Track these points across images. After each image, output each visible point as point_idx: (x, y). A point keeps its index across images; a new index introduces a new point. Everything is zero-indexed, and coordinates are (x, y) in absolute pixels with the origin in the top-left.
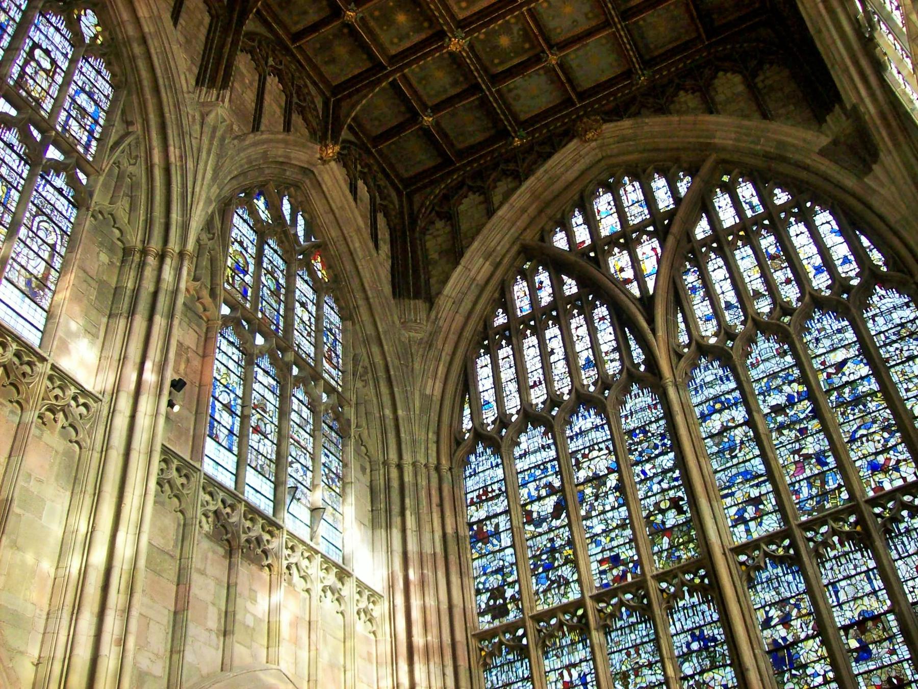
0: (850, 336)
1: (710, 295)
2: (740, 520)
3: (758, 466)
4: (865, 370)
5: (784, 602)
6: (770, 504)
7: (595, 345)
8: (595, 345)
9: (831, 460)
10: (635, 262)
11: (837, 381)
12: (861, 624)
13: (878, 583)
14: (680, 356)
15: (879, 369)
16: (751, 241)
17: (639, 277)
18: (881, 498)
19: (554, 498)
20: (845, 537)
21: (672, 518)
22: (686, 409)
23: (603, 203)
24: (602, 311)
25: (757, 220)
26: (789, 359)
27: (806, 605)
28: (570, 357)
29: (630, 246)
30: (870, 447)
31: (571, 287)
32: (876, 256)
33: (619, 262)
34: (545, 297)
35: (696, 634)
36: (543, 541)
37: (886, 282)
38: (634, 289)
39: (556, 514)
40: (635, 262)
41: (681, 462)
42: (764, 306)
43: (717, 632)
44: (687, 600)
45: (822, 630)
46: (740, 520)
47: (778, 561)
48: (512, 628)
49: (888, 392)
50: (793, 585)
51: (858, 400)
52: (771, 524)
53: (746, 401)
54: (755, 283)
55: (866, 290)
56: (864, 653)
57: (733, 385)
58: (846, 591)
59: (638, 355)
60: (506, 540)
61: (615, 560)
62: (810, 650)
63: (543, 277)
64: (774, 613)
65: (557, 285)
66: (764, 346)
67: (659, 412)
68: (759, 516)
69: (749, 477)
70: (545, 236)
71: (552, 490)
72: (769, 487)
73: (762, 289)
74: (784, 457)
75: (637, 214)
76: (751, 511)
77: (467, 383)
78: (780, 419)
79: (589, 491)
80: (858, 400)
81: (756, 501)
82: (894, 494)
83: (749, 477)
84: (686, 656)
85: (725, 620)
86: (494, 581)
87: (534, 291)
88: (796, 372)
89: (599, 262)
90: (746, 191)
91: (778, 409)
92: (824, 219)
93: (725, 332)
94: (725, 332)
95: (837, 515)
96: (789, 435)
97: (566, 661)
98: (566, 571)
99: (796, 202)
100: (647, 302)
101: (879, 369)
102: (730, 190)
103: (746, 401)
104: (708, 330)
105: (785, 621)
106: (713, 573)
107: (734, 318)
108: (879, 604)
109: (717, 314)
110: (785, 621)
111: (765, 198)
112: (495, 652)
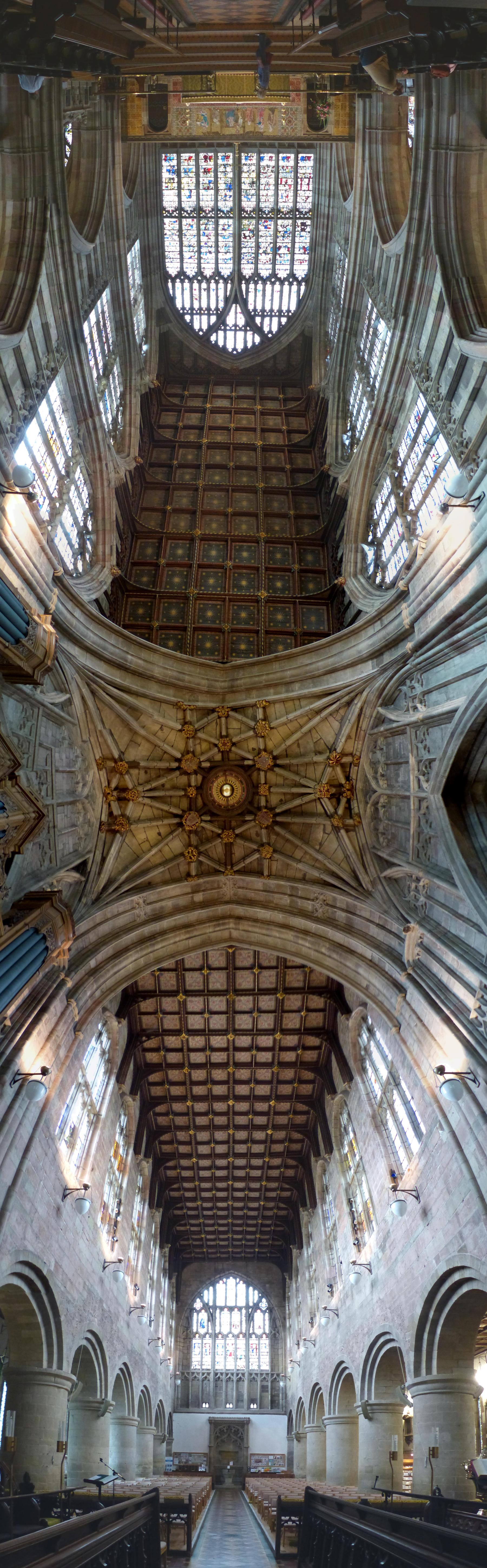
0: (185, 265)
1: (217, 297)
2: (229, 226)
3: (220, 239)
4: (184, 254)
5: (225, 200)
6: (220, 228)
7: (256, 296)
8: (256, 296)
9: (201, 232)
10: (236, 318)
11: (192, 254)
12: (208, 188)
13: (201, 197)
14: (231, 280)
15: (181, 253)
16: (200, 309)
17: (236, 313)
18: (193, 217)
19: (280, 252)
20: (205, 211)
21: (247, 233)
22: (234, 263)
23: (240, 347)
24: (251, 307)
25: (197, 314)
26: (203, 265)
27: (219, 198)
28: (264, 295)
29: (236, 325)
30: (191, 232)
31: (258, 320)
32: (170, 285)
33: (241, 321)
34: (267, 320)
35: (249, 200)
36: (286, 240)
37: (170, 276)
38: (239, 310)
39: (280, 248)
40: (236, 318)
41: (240, 248)
42: (204, 285)
43: (243, 198)
44: (249, 209)
45: (217, 190)
46: (229, 226)
47: (223, 212)
48: (300, 218)
49: (181, 245)
50: (221, 204)
51: (190, 246)
52: (222, 222)
53: (217, 259)
54: (204, 294)
55: (177, 276)
56: (210, 182)
57: (220, 266)
58: (209, 198)
59: (244, 286)
60: (297, 245)
61: (266, 227)
62: (222, 186)
63: (266, 329)
64: (228, 198)
65: (262, 323)
66: (208, 272)
67: (242, 266)
68: (224, 225)
69: (224, 236)
70: (262, 342)
71: (279, 255)
72: (220, 232)
73: (202, 291)
74: (213, 239)
75: (230, 334)
76: (226, 227)
77: (300, 302)
78: (210, 249)
79: (269, 251)
80: (190, 246)
81: (224, 229)
82: (189, 217)
83: (224, 236)
84: (253, 195)
85: (240, 201)
86: (303, 233)
87: (270, 325)
88: (202, 261)
89: (247, 324)
90: (196, 326)
91: (210, 252)
92: (179, 305)
93: (217, 282)
94: (217, 282)
95: (204, 217)
96: (210, 244)
97: (286, 204)
98: (280, 229)
99: (184, 314)
100: (236, 301)
101: (181, 253)
102: (201, 329)
103: (217, 259)
104: (221, 285)
105: (226, 195)
106: (240, 214)
107: (213, 285)
108: (202, 192)
109: (217, 289)
110: (226, 195)
111: (192, 320)
112: (306, 213)
